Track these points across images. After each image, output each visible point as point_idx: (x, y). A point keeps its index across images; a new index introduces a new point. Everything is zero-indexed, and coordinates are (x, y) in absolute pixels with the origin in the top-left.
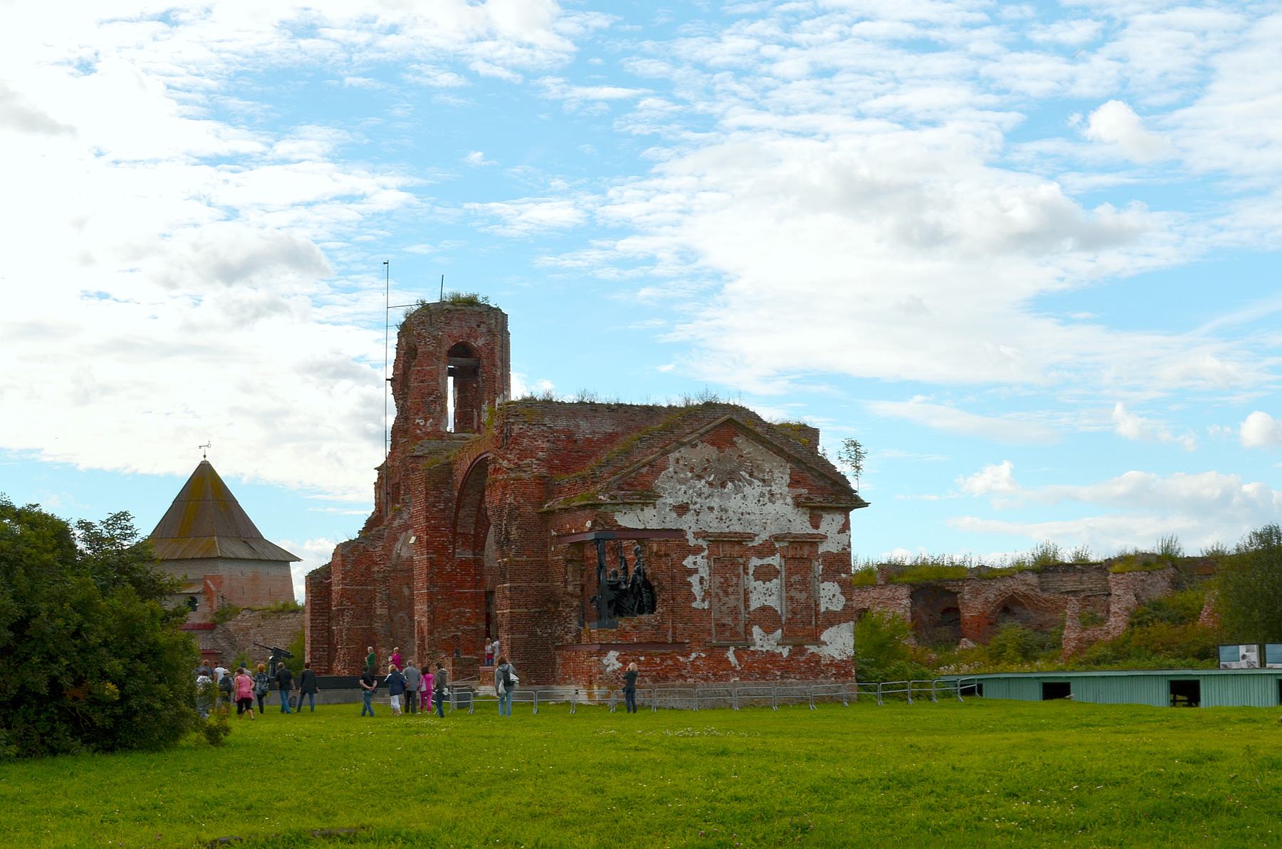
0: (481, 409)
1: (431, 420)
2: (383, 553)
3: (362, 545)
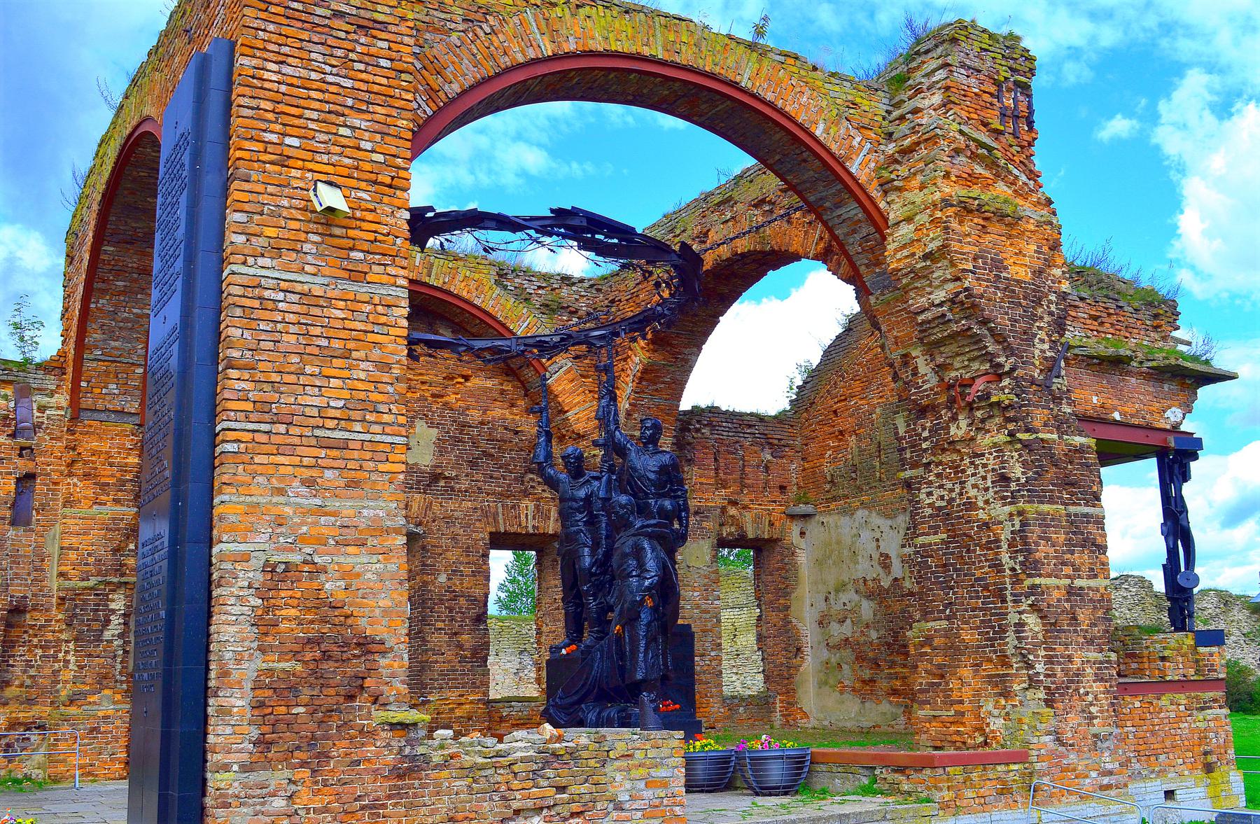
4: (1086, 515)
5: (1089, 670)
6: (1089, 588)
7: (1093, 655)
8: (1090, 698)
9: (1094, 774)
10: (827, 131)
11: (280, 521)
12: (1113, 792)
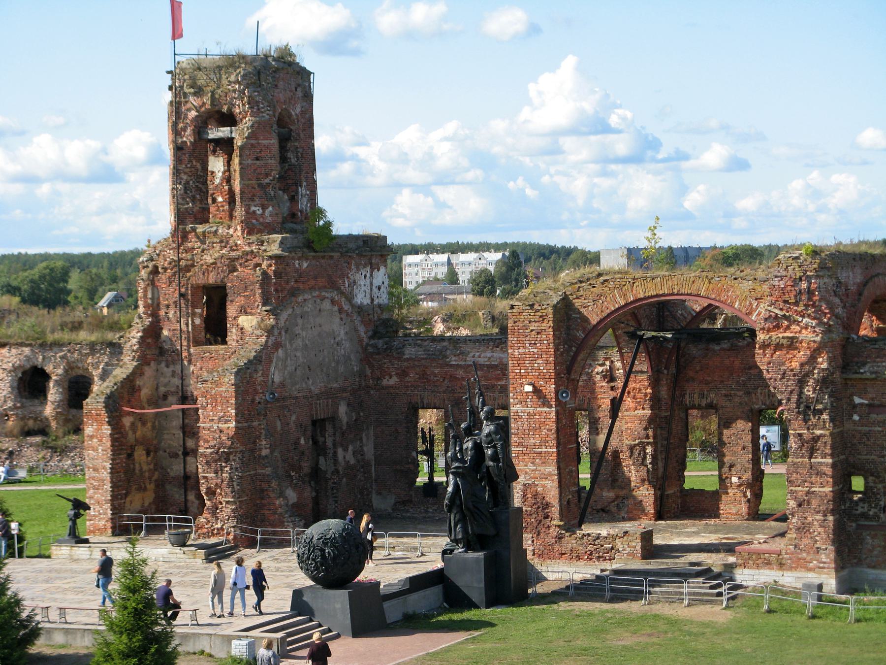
0: (297, 192)
1: (270, 209)
2: (262, 378)
3: (249, 371)
4: (819, 463)
5: (815, 523)
6: (819, 491)
7: (820, 517)
8: (816, 533)
9: (815, 562)
10: (740, 304)
11: (526, 473)
12: (825, 570)
